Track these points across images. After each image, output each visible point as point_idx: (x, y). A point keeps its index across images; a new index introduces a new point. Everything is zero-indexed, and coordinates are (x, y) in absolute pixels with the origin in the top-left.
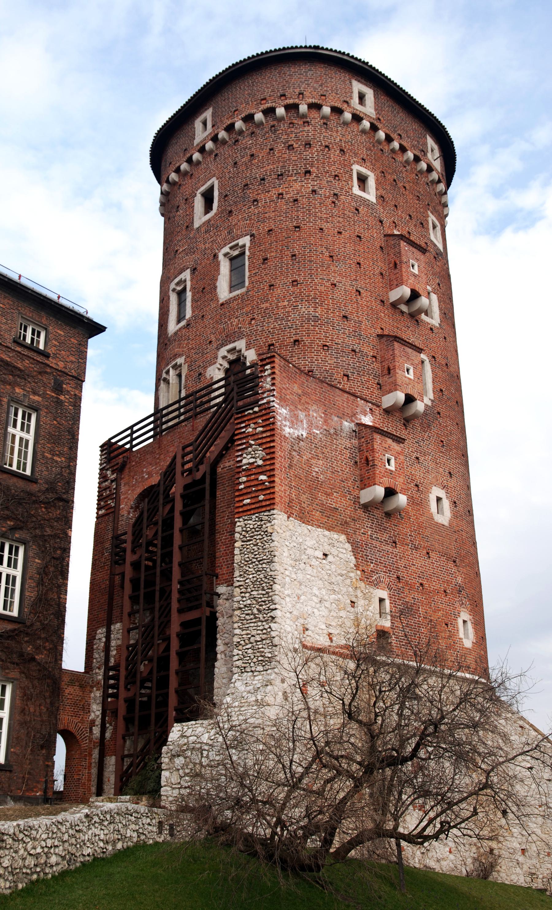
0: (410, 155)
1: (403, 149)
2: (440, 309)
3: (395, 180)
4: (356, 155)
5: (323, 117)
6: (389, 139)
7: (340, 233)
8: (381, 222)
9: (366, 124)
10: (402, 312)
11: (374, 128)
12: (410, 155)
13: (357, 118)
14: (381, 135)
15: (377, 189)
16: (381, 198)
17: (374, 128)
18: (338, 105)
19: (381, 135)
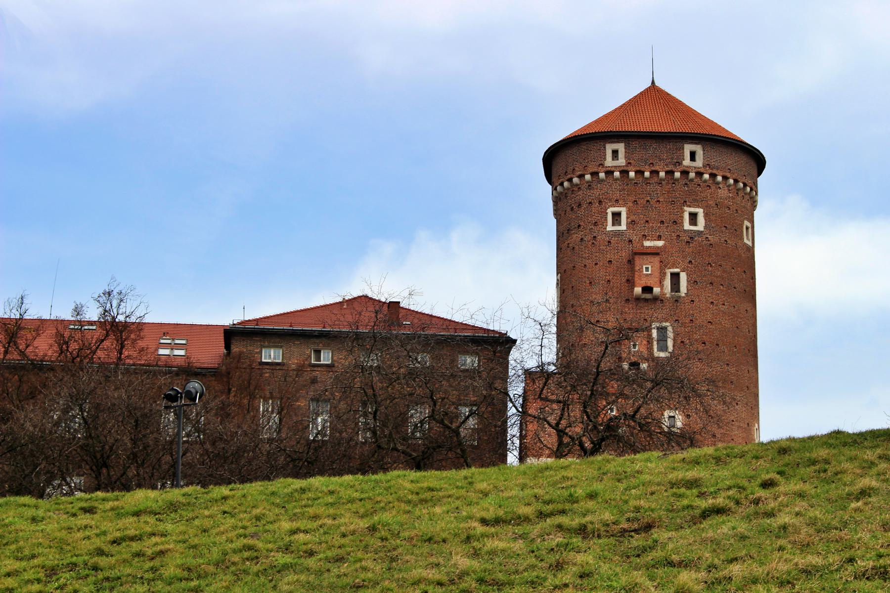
0: (662, 174)
1: (655, 173)
2: (688, 281)
3: (648, 201)
4: (610, 200)
5: (587, 182)
6: (640, 173)
7: (596, 264)
8: (630, 241)
9: (617, 174)
10: (646, 300)
11: (624, 173)
12: (662, 174)
13: (609, 173)
14: (632, 174)
15: (627, 218)
16: (631, 223)
17: (624, 173)
18: (595, 170)
19: (632, 174)
